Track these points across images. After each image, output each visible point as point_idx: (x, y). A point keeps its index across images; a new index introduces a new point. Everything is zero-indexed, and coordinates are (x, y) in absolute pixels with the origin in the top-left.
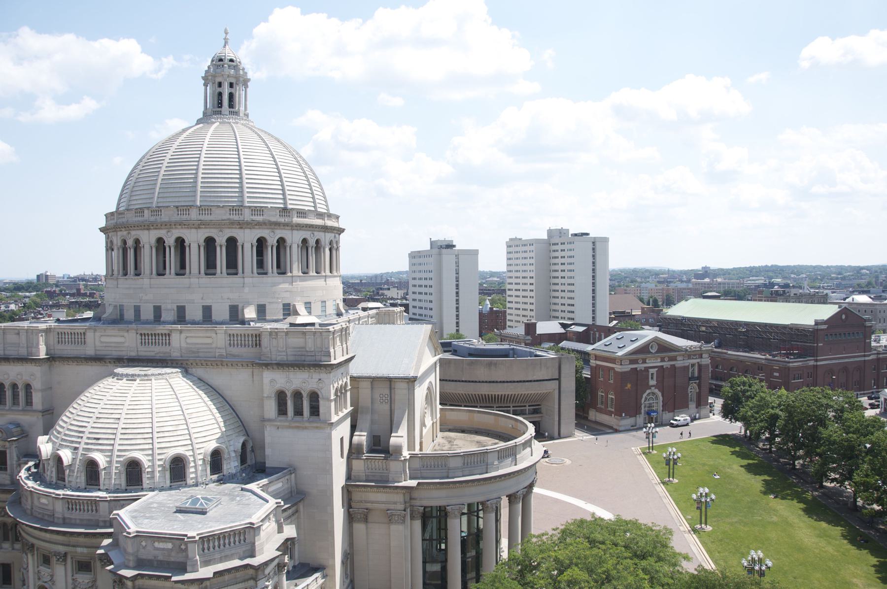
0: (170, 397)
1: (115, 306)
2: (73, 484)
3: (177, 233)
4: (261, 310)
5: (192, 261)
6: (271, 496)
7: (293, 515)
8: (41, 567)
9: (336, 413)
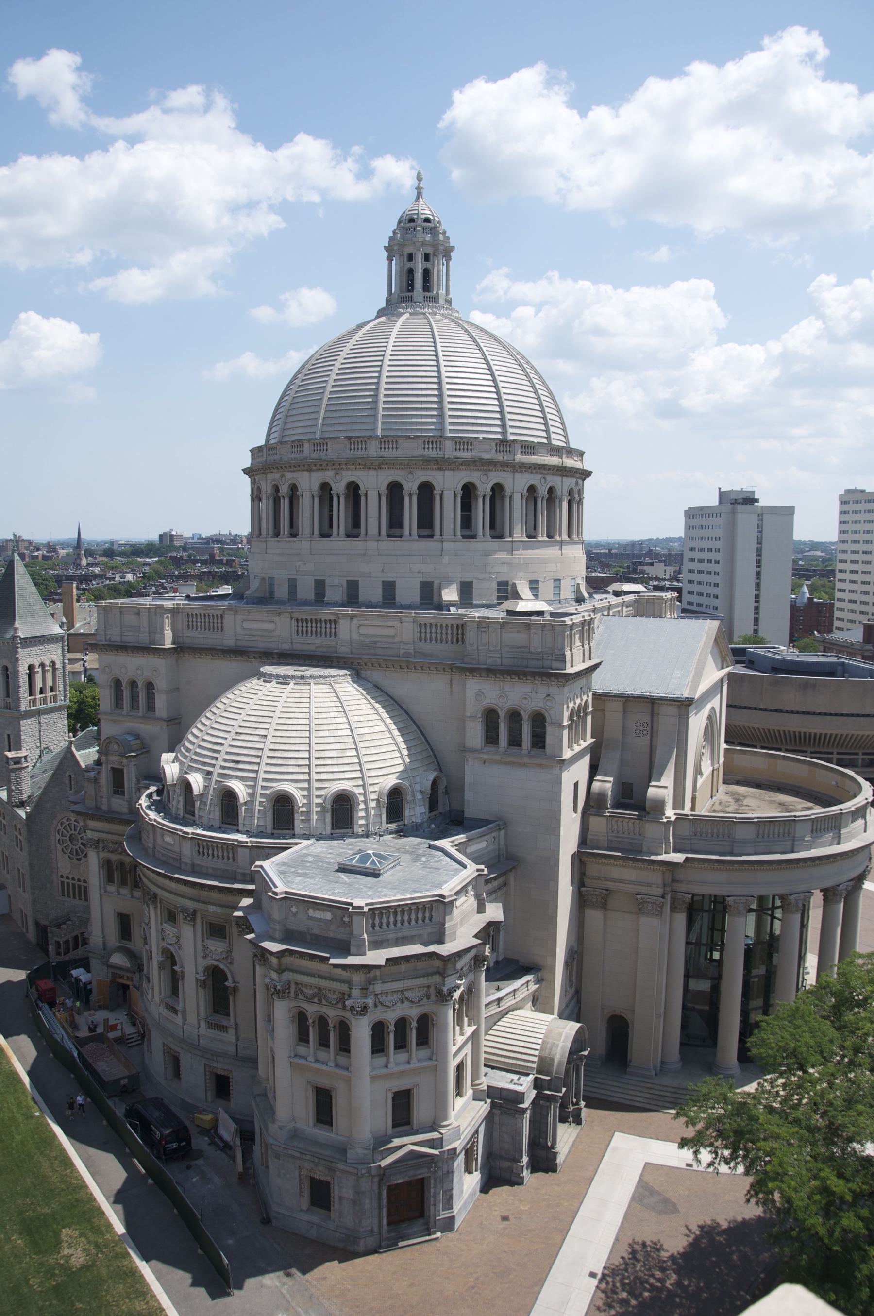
0: (334, 709)
1: (263, 579)
2: (205, 821)
3: (349, 476)
4: (466, 591)
5: (369, 515)
6: (470, 859)
7: (499, 888)
9: (570, 747)
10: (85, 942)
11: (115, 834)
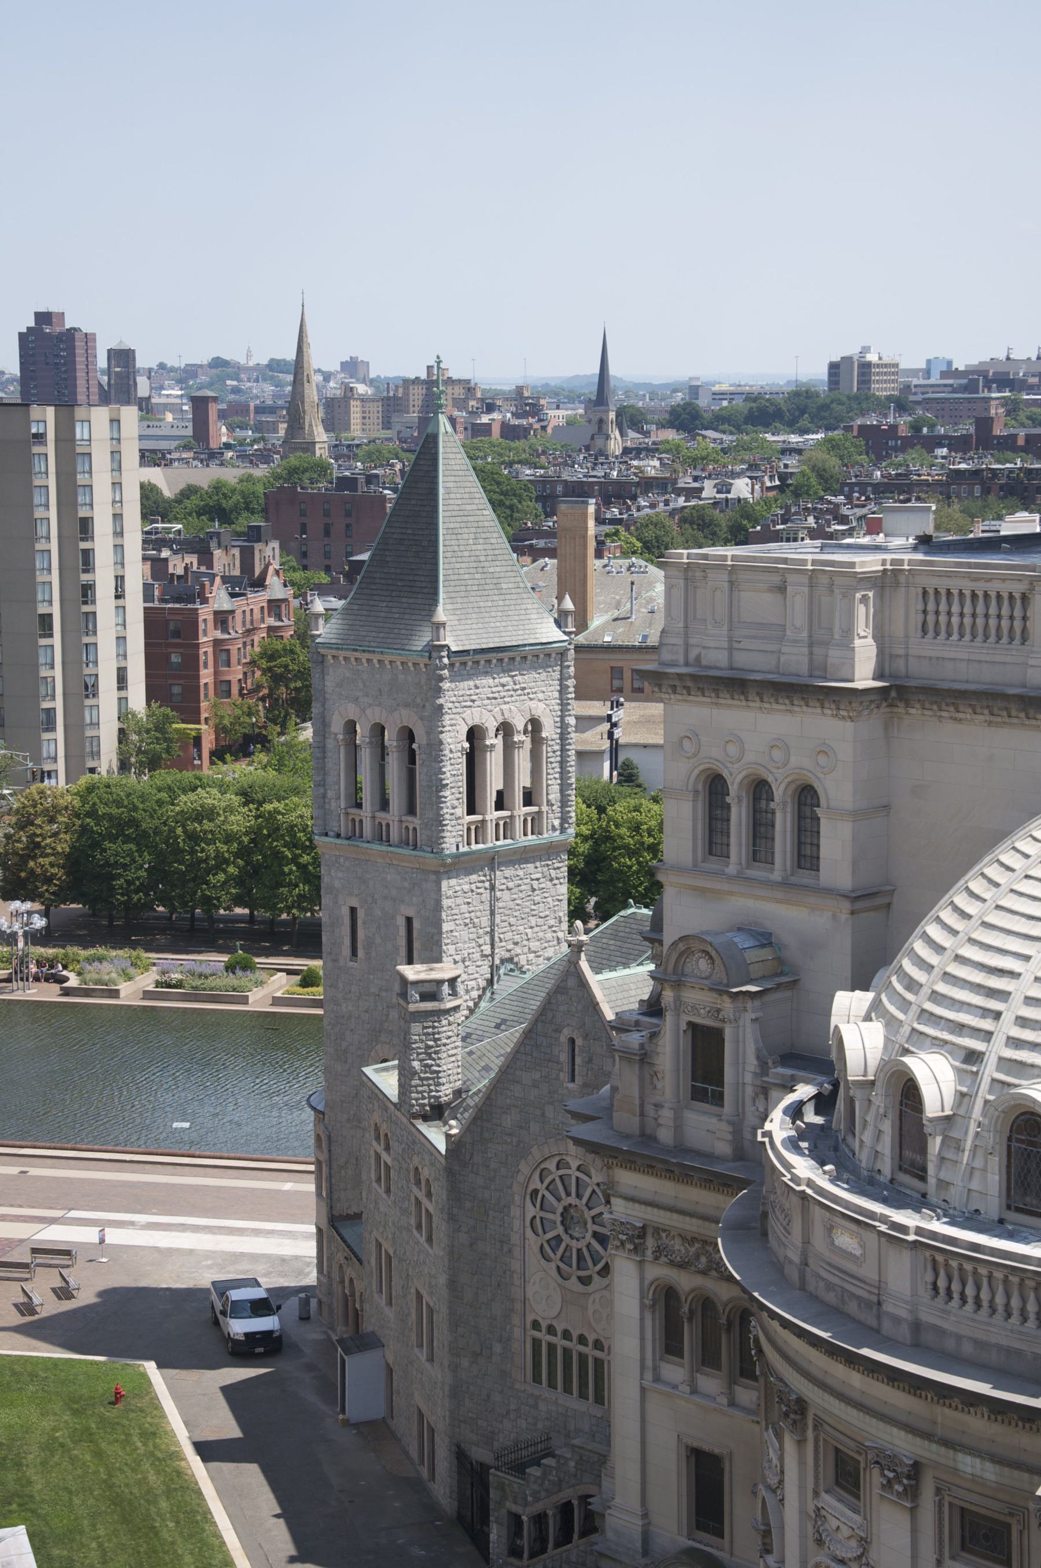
2: (955, 1196)
8: (824, 1495)
10: (592, 1525)
11: (691, 1215)
